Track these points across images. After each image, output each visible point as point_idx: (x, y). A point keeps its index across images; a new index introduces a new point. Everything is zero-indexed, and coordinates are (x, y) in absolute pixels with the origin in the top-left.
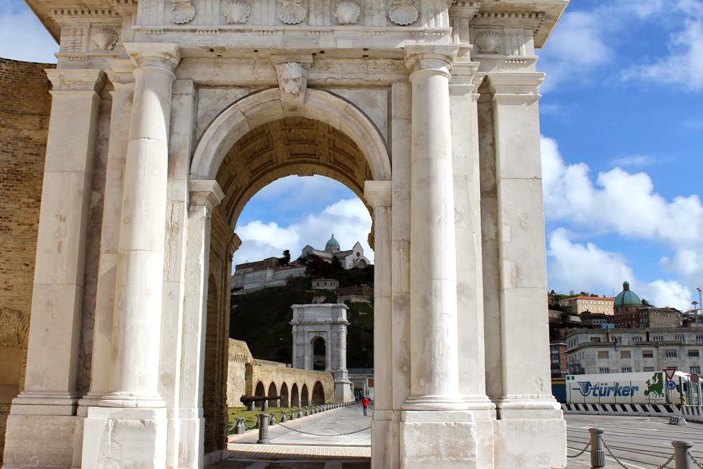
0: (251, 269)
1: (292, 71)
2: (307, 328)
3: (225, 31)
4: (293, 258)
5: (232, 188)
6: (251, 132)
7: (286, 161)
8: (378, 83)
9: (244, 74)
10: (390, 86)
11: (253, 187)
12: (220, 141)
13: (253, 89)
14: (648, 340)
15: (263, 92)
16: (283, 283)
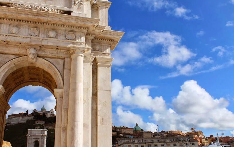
0: (14, 117)
1: (32, 51)
2: (33, 137)
3: (10, 36)
4: (29, 113)
5: (8, 89)
6: (17, 70)
7: (28, 80)
8: (61, 57)
9: (16, 51)
10: (65, 58)
11: (16, 89)
12: (5, 72)
13: (18, 56)
14: (143, 141)
15: (22, 57)
16: (25, 121)
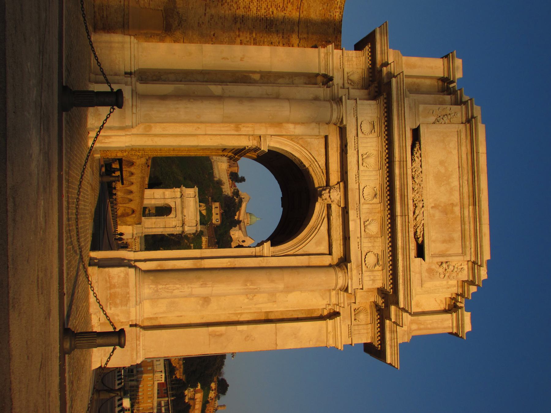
2: (178, 201)
4: (239, 185)
